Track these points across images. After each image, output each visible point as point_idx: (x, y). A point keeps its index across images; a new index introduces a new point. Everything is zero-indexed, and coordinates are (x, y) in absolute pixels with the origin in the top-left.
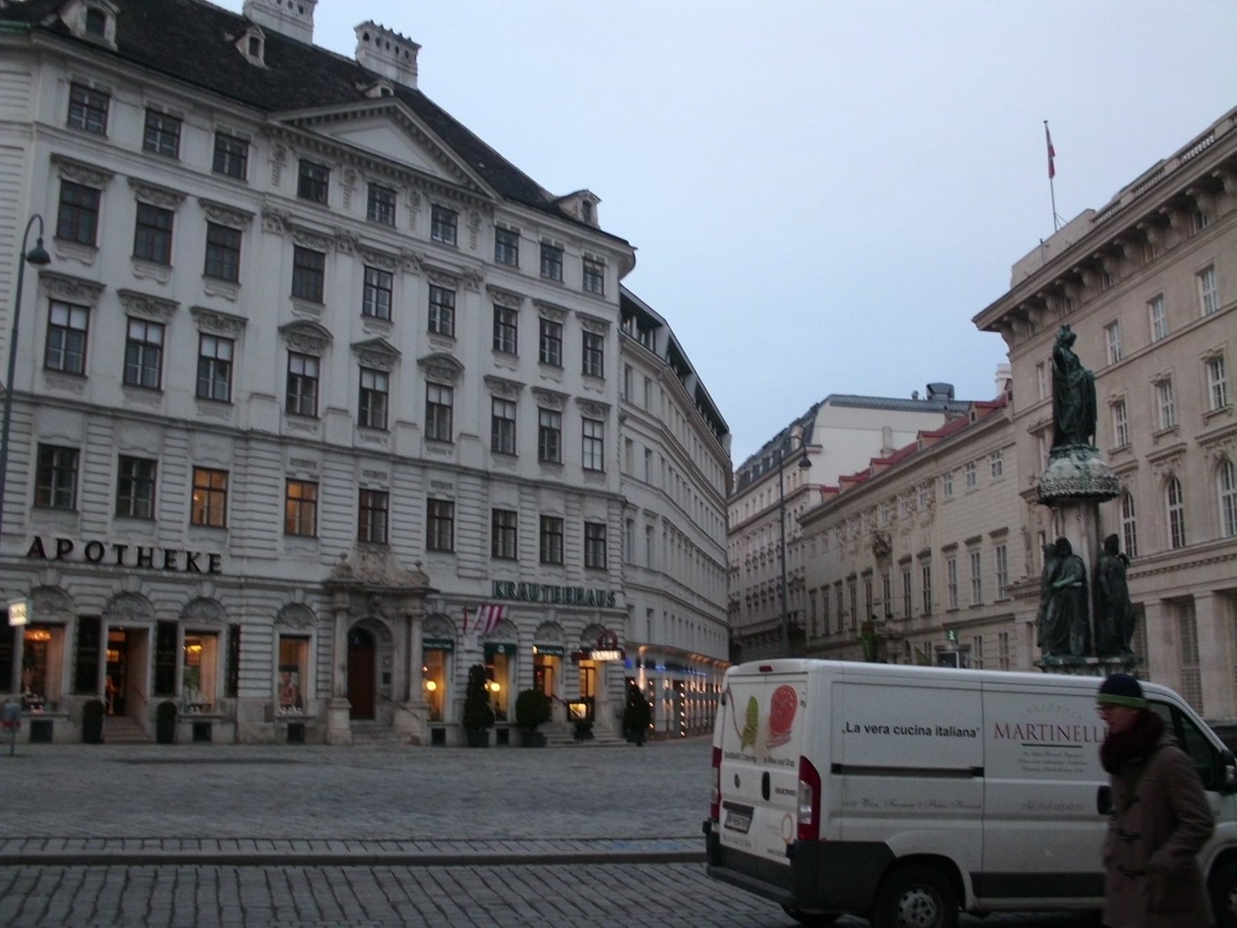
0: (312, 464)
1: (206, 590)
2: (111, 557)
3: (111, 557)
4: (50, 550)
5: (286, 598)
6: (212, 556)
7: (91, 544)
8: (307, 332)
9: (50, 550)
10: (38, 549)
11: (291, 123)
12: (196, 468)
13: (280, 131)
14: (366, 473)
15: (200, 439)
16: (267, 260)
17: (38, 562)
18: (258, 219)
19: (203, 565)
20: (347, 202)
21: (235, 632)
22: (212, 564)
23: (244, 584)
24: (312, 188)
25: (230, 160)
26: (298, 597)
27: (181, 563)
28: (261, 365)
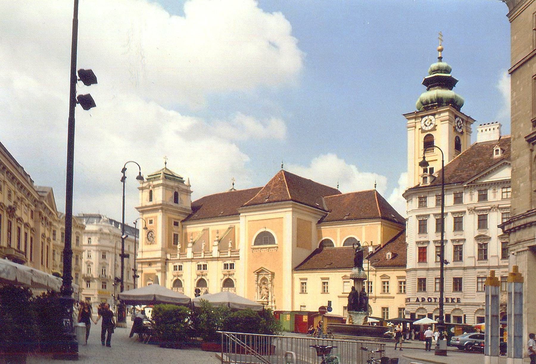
0: (485, 272)
1: (457, 307)
2: (433, 300)
3: (433, 300)
4: (420, 300)
5: (478, 308)
6: (458, 299)
7: (429, 298)
8: (482, 237)
9: (420, 300)
10: (418, 300)
11: (471, 182)
12: (436, 279)
13: (468, 186)
14: (502, 272)
15: (454, 271)
16: (470, 222)
17: (418, 303)
18: (467, 212)
19: (456, 301)
20: (495, 196)
21: (465, 316)
22: (458, 301)
23: (465, 305)
24: (483, 197)
25: (458, 200)
26: (481, 307)
27: (450, 301)
28: (470, 249)
